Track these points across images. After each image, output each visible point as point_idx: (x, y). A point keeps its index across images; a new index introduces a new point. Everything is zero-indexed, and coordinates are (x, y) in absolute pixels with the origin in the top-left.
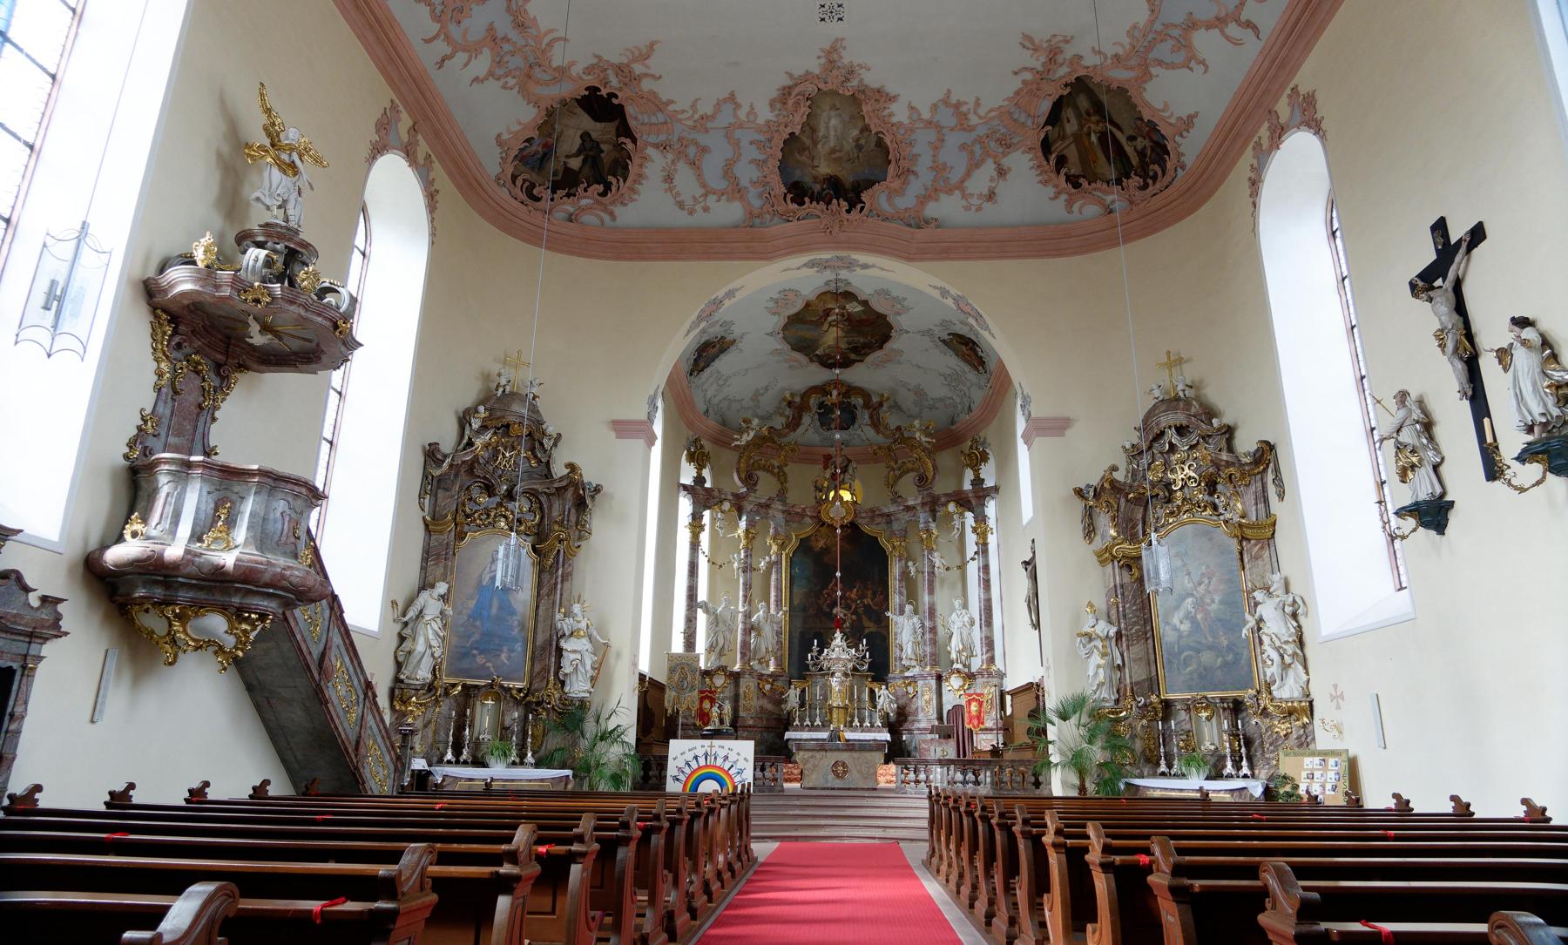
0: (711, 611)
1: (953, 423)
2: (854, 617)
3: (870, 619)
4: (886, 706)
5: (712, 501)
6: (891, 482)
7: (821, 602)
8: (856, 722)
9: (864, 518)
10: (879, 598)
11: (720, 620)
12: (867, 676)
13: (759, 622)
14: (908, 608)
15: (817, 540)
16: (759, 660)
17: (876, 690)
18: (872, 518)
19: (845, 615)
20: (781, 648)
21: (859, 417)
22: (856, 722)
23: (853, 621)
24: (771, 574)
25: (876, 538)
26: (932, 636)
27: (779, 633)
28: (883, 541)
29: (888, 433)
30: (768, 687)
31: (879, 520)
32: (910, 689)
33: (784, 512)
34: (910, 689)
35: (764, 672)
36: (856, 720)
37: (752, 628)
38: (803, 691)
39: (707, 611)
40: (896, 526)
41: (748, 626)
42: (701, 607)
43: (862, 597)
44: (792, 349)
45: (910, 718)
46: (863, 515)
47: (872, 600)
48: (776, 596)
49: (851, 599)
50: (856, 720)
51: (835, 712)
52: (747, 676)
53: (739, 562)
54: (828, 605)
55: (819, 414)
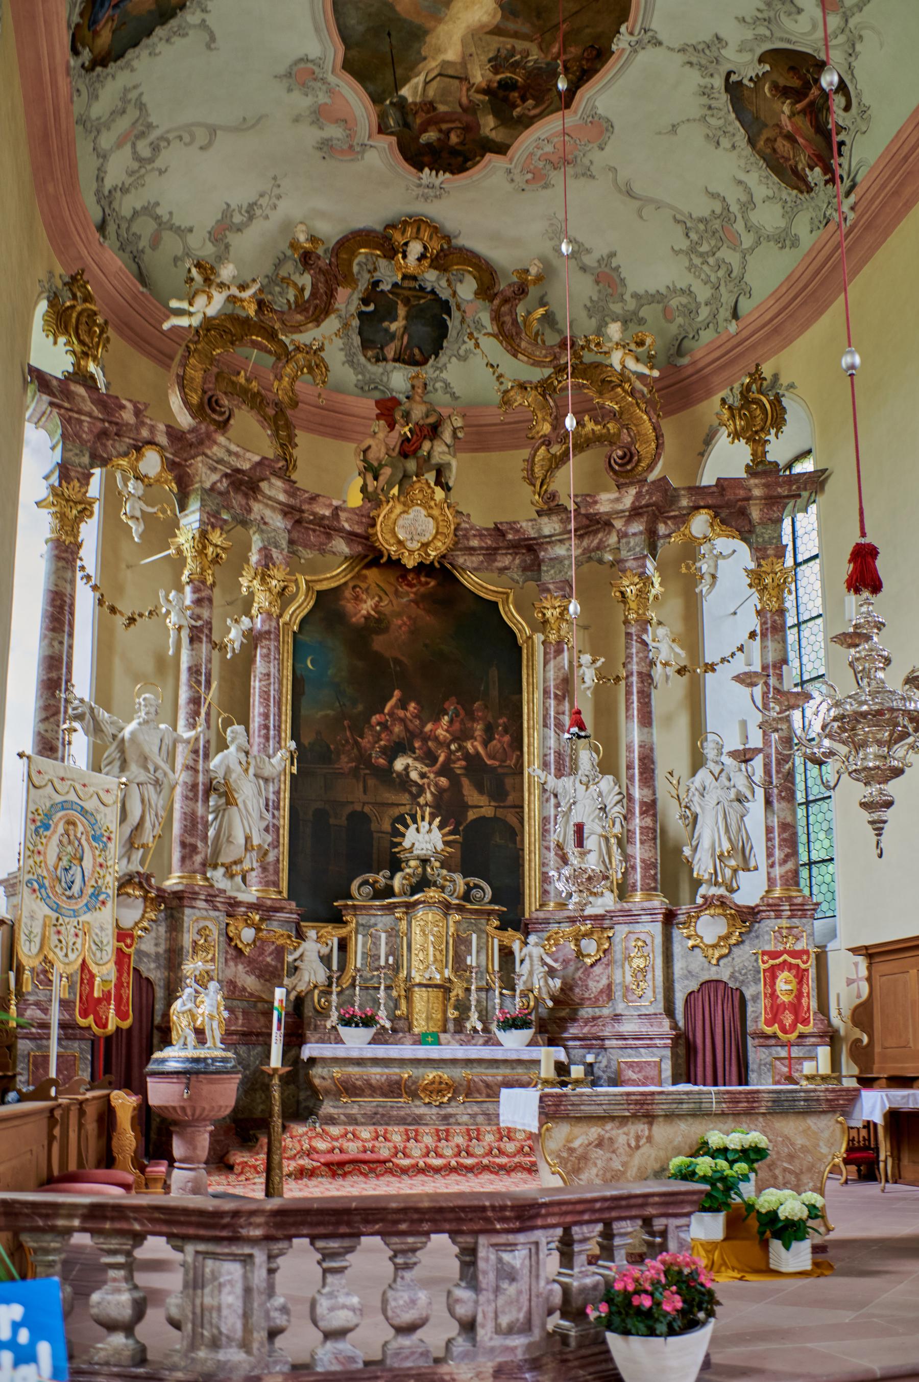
0: (110, 730)
1: (680, 352)
2: (443, 781)
3: (480, 789)
4: (538, 983)
5: (113, 446)
6: (539, 472)
7: (365, 742)
8: (474, 1021)
9: (471, 550)
10: (501, 740)
11: (131, 755)
12: (490, 913)
13: (228, 771)
14: (586, 758)
15: (357, 598)
16: (227, 867)
17: (516, 946)
18: (491, 553)
19: (423, 775)
20: (276, 844)
21: (452, 333)
22: (474, 1021)
23: (441, 791)
24: (252, 660)
25: (496, 604)
26: (648, 821)
27: (272, 806)
28: (512, 615)
29: (539, 353)
30: (248, 934)
31: (504, 560)
32: (590, 946)
33: (288, 511)
34: (590, 946)
35: (242, 897)
36: (474, 1016)
37: (210, 788)
38: (343, 945)
39: (96, 729)
40: (548, 576)
41: (201, 778)
42: (79, 717)
43: (462, 736)
44: (348, 66)
45: (586, 1012)
46: (475, 543)
47: (485, 744)
48: (266, 716)
49: (436, 739)
50: (474, 1016)
51: (420, 996)
52: (201, 904)
53: (182, 610)
54: (384, 751)
55: (361, 314)
